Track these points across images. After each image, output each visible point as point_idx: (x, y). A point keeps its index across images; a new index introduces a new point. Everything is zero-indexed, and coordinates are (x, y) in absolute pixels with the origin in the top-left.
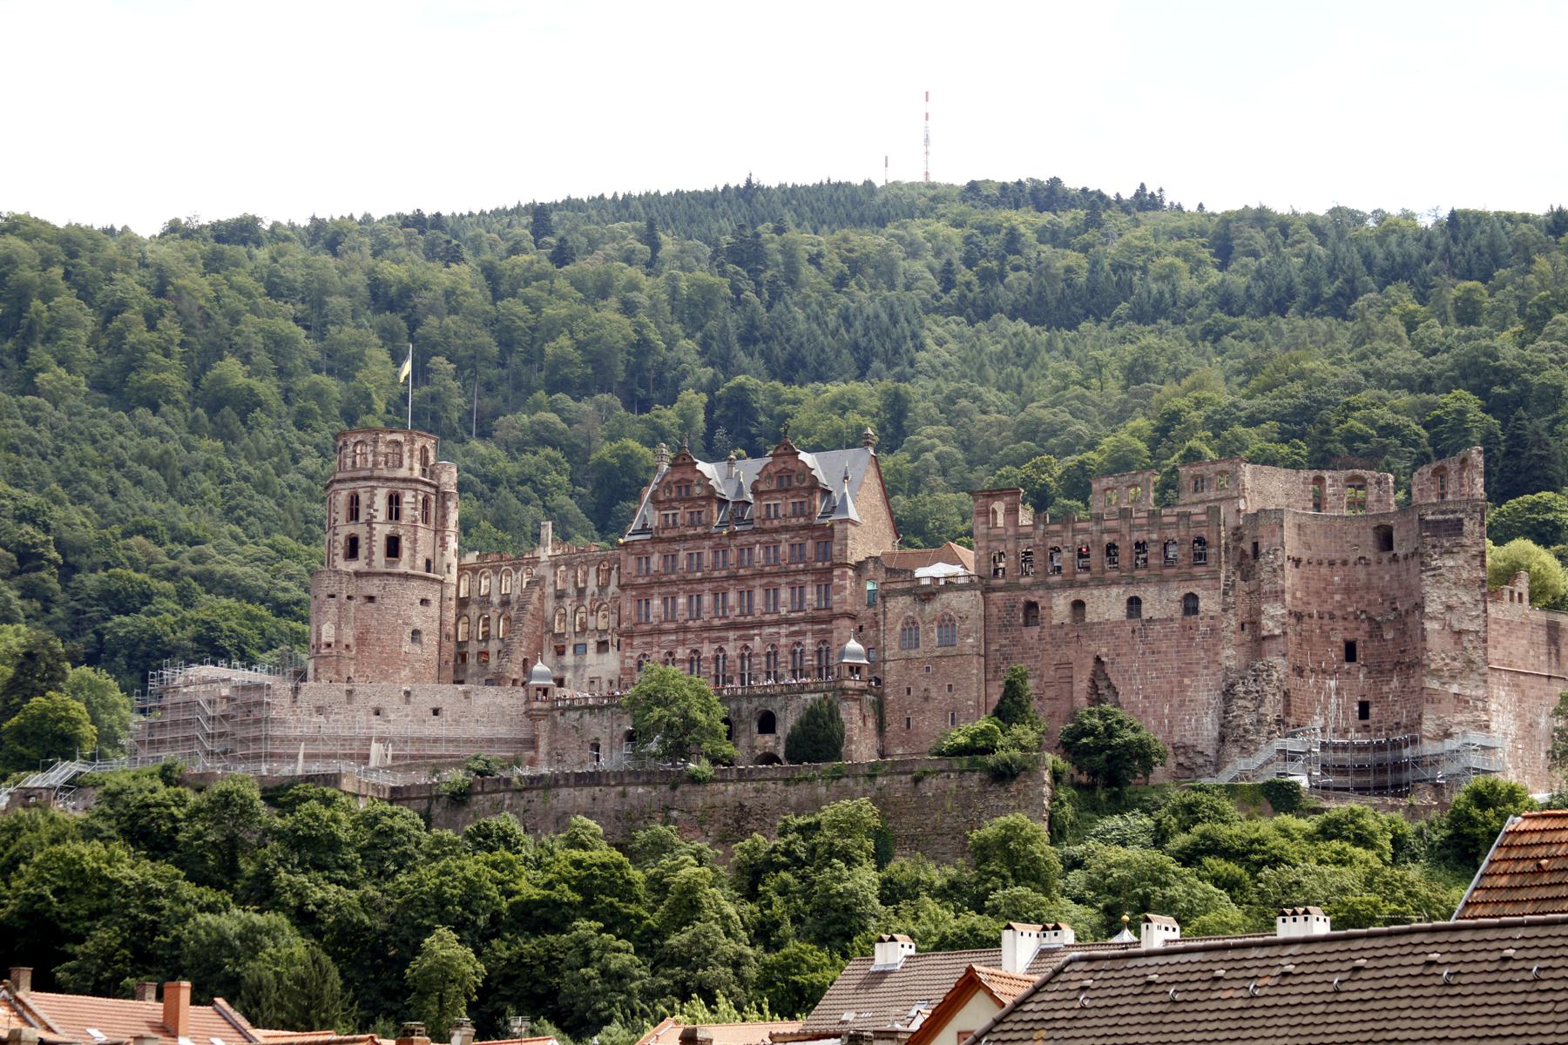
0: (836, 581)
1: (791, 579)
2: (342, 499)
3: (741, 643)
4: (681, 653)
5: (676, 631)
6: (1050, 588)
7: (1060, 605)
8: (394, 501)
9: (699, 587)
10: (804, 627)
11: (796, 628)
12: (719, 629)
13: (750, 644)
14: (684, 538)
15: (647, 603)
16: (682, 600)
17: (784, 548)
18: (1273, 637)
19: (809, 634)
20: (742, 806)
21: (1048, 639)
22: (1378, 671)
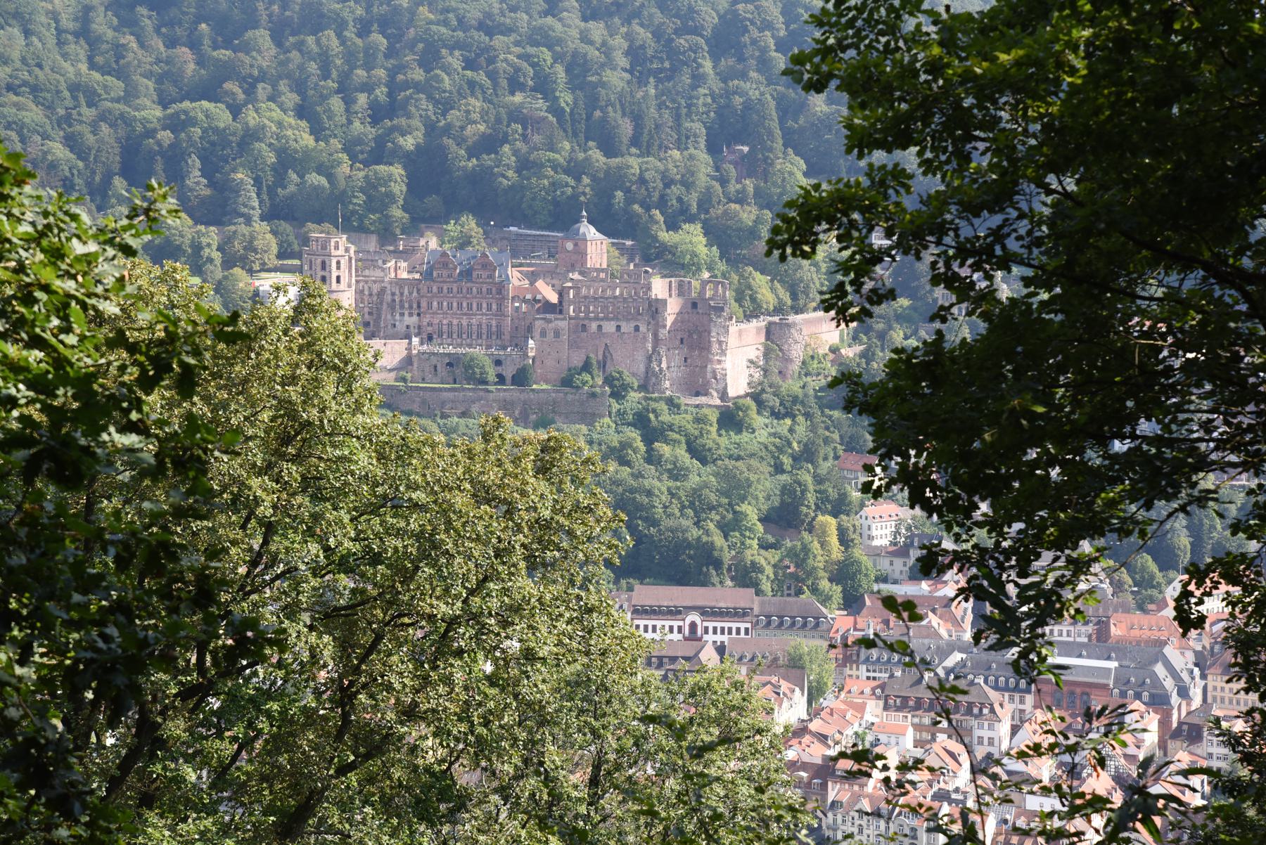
2: (319, 261)
4: (445, 322)
6: (590, 319)
8: (338, 263)
14: (444, 282)
17: (484, 290)
22: (691, 348)
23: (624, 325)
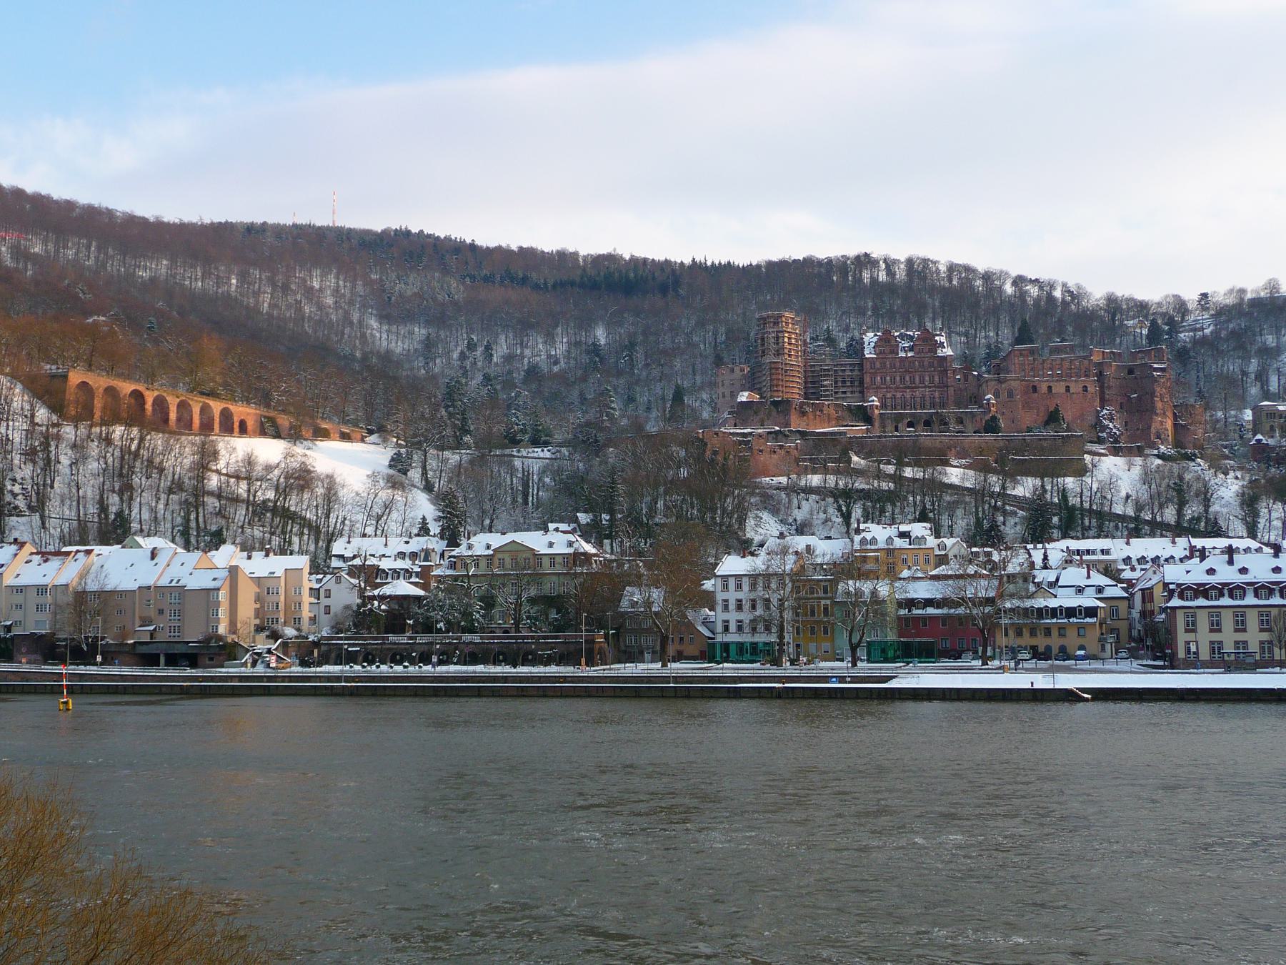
7: (1043, 388)
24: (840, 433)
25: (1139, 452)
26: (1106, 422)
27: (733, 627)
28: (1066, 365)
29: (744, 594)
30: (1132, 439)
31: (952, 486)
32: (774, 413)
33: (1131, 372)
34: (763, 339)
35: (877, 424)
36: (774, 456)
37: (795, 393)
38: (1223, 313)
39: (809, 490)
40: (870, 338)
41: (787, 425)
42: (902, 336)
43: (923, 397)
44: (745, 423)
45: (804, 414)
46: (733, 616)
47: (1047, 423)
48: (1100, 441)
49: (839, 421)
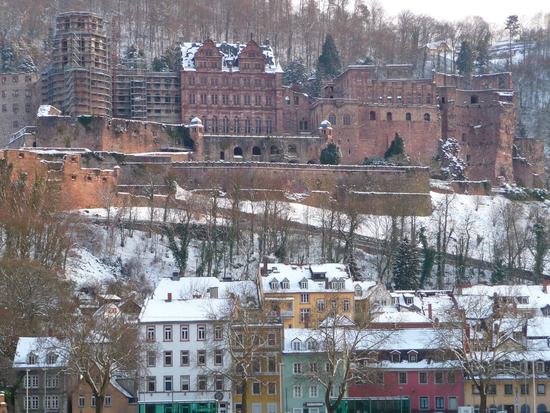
0: (278, 95)
1: (256, 93)
3: (235, 115)
5: (207, 108)
7: (383, 115)
9: (217, 92)
10: (261, 111)
11: (258, 112)
12: (226, 109)
13: (238, 116)
15: (194, 96)
16: (209, 96)
18: (451, 131)
19: (264, 115)
20: (319, 180)
21: (379, 125)
23: (414, 113)
24: (164, 159)
25: (486, 190)
26: (449, 155)
27: (177, 385)
28: (408, 89)
29: (208, 345)
30: (476, 175)
31: (296, 225)
32: (82, 131)
33: (474, 100)
34: (65, 43)
35: (200, 149)
36: (89, 183)
37: (101, 106)
38: (532, 39)
39: (134, 225)
40: (188, 49)
41: (98, 146)
42: (225, 48)
43: (248, 120)
44: (46, 142)
45: (117, 134)
46: (176, 370)
47: (388, 154)
48: (444, 177)
49: (157, 144)
